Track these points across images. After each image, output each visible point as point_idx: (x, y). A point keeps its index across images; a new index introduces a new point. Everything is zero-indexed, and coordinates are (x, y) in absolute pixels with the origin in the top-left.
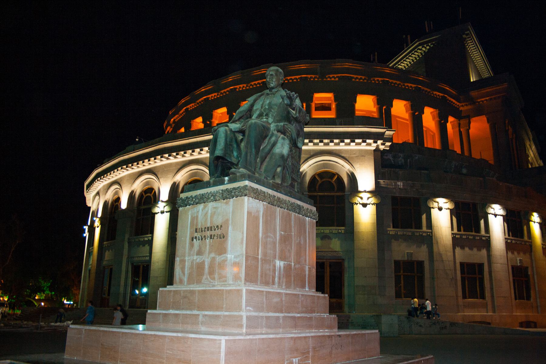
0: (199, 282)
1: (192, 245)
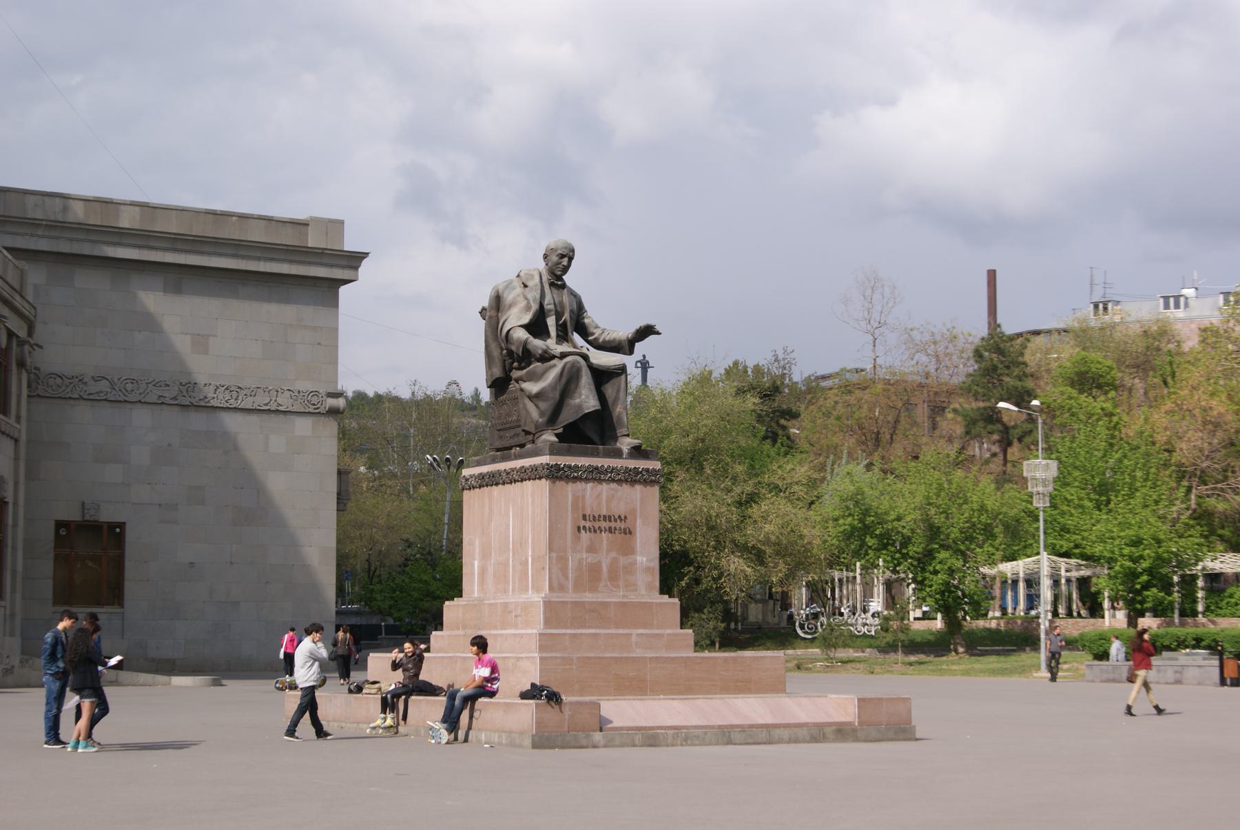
0: (593, 589)
1: (577, 539)
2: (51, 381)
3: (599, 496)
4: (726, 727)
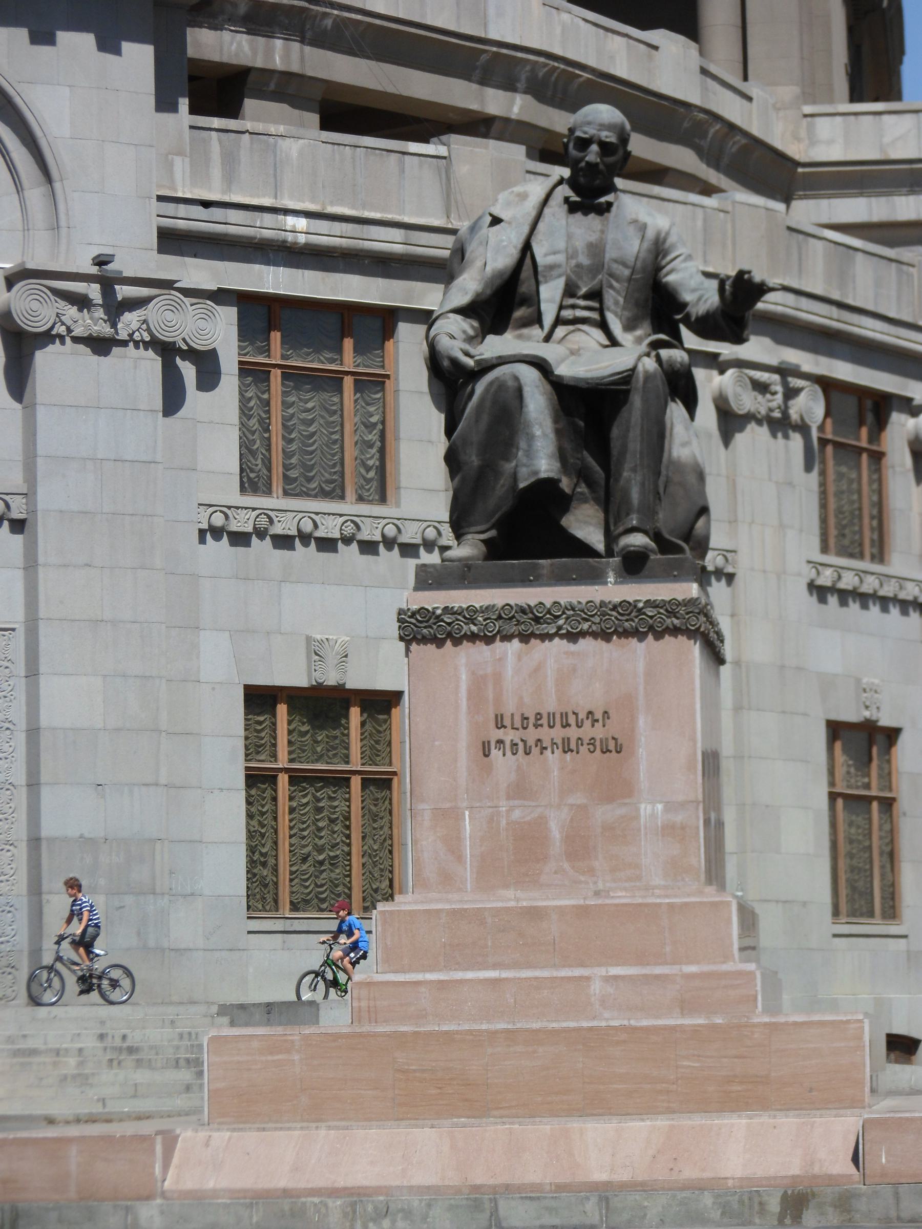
3: (538, 669)
4: (494, 1189)
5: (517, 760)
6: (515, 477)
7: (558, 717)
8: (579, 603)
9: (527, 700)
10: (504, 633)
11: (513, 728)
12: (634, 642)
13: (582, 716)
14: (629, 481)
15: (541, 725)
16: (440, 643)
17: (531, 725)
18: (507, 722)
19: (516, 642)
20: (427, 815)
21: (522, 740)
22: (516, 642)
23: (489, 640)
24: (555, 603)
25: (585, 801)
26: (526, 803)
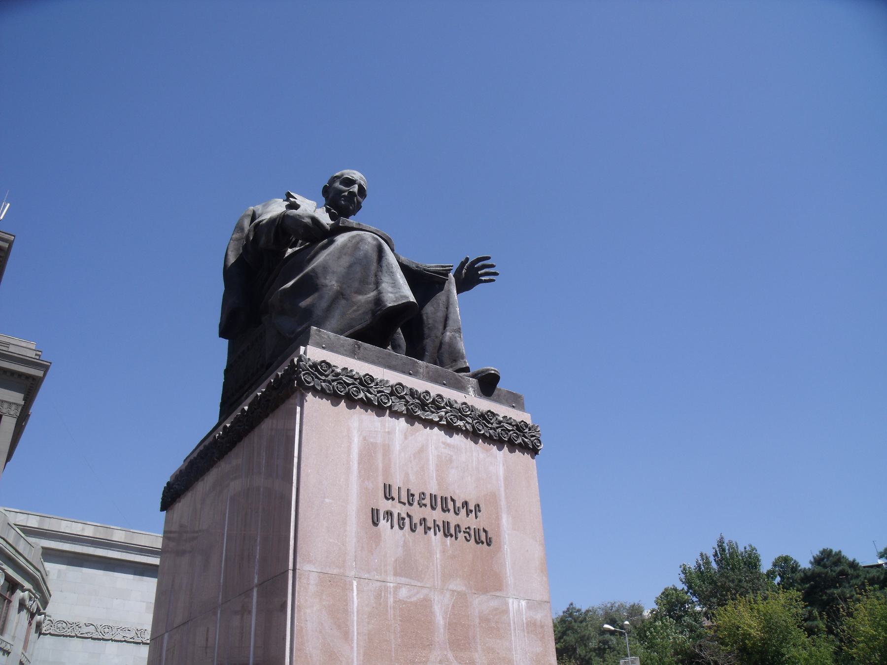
2: (60, 625)
3: (422, 450)
5: (404, 535)
6: (378, 301)
7: (439, 500)
8: (456, 402)
9: (412, 477)
10: (396, 408)
11: (400, 502)
12: (494, 448)
13: (459, 504)
14: (453, 338)
15: (425, 505)
16: (335, 403)
17: (416, 503)
18: (395, 494)
19: (402, 420)
20: (313, 579)
21: (409, 516)
22: (402, 420)
23: (380, 409)
24: (438, 395)
25: (464, 589)
26: (413, 582)
